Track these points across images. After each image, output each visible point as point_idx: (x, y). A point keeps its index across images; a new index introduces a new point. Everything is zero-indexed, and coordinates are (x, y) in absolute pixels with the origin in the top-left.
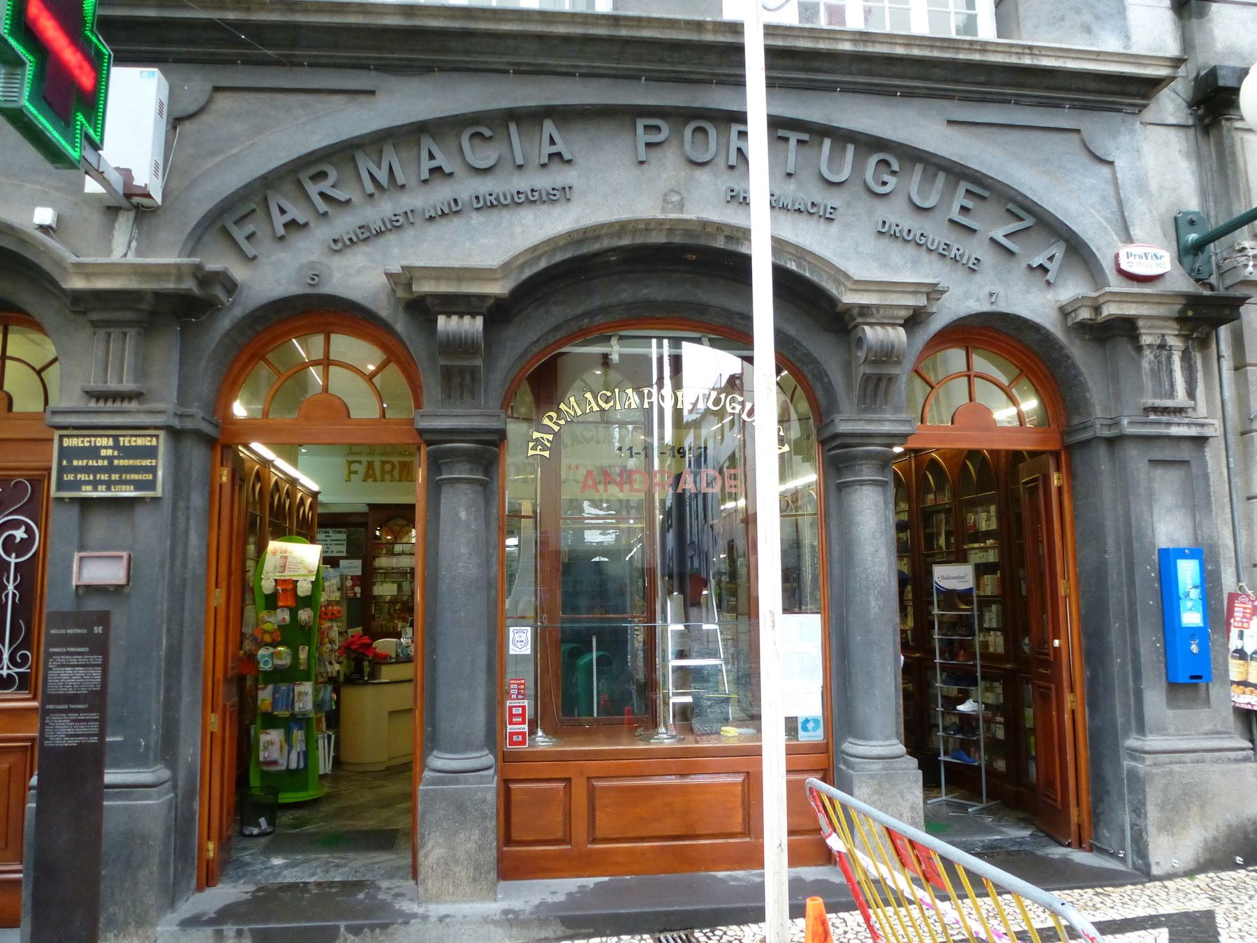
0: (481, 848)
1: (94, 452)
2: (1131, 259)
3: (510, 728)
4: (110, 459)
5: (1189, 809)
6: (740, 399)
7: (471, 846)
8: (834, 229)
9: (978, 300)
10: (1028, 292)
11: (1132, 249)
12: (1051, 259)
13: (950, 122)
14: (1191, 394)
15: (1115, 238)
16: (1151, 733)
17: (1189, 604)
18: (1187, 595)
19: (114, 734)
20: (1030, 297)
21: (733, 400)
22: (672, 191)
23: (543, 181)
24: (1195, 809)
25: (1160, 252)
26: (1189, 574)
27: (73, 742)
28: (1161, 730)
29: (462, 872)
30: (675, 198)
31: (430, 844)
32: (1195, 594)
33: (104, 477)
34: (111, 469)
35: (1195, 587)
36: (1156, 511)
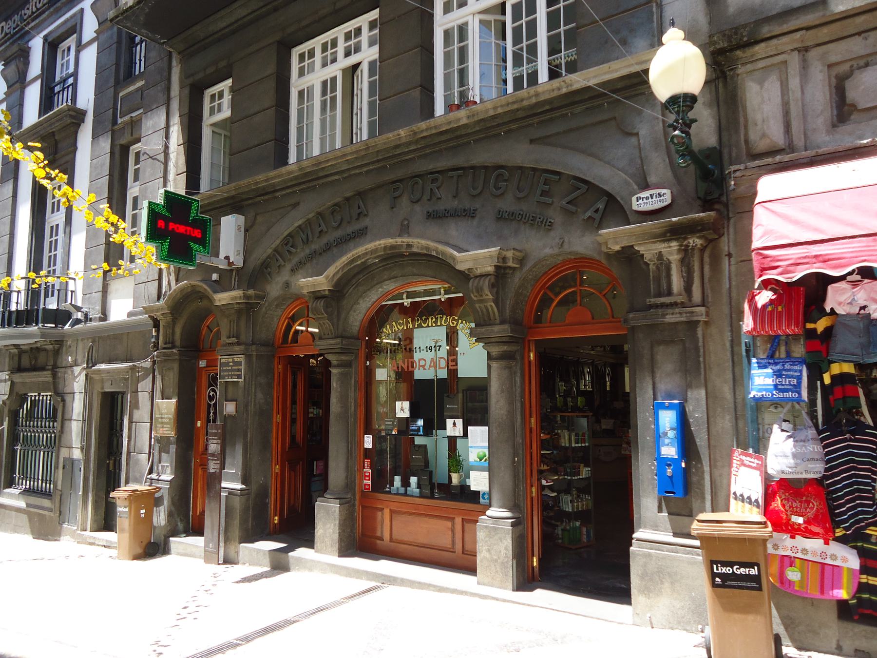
0: (334, 532)
1: (227, 364)
2: (640, 202)
3: (365, 482)
5: (662, 583)
7: (331, 531)
8: (475, 222)
9: (552, 247)
10: (583, 236)
12: (596, 211)
13: (532, 141)
14: (688, 289)
15: (635, 187)
16: (645, 527)
17: (667, 441)
18: (666, 434)
20: (584, 239)
22: (405, 219)
23: (356, 226)
24: (667, 585)
25: (663, 191)
26: (667, 419)
27: (213, 471)
28: (655, 527)
29: (328, 541)
30: (406, 223)
32: (671, 434)
34: (232, 370)
35: (672, 429)
36: (658, 375)
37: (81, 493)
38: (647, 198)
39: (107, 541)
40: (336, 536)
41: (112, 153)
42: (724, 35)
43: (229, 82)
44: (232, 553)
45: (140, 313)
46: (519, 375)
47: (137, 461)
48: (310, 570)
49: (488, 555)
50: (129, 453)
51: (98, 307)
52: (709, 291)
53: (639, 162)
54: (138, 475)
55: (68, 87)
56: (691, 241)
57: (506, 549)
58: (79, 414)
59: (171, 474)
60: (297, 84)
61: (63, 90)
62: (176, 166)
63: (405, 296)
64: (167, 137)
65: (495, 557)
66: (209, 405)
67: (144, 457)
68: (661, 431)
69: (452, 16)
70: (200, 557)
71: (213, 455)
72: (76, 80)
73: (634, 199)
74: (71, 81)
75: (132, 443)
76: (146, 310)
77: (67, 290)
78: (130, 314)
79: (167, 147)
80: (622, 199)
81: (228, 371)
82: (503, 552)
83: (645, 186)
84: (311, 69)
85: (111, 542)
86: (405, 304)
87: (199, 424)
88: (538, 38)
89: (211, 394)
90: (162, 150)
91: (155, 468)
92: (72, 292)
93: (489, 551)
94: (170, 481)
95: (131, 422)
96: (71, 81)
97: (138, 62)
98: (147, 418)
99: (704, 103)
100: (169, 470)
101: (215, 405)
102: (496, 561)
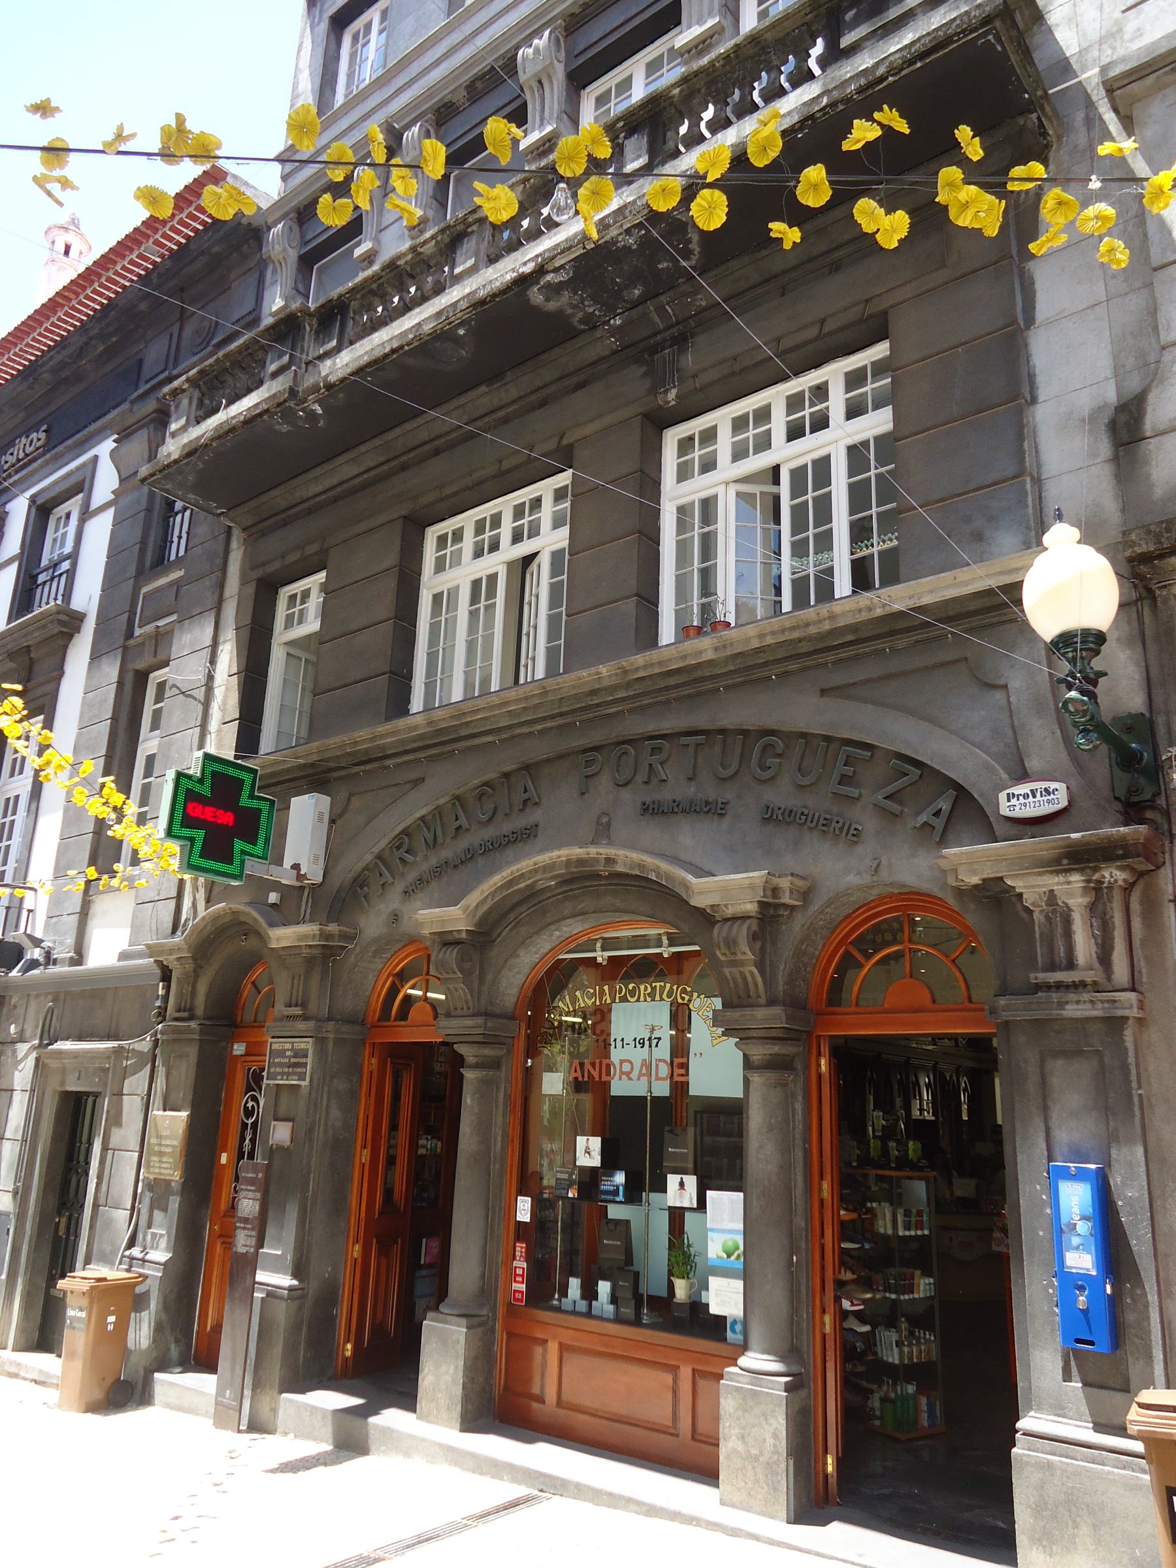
2: (1014, 801)
3: (515, 1286)
4: (290, 1057)
5: (1076, 1526)
6: (689, 989)
7: (449, 1378)
8: (726, 823)
9: (859, 873)
11: (1024, 789)
12: (937, 814)
13: (823, 692)
14: (1105, 958)
15: (1005, 776)
16: (1039, 1409)
17: (1075, 1241)
19: (270, 1247)
21: (684, 991)
24: (1085, 1530)
25: (1053, 785)
28: (1059, 1410)
30: (605, 820)
31: (426, 1370)
32: (1083, 1228)
33: (286, 1070)
35: (1084, 1218)
36: (1055, 1115)
37: (4, 1277)
38: (1026, 796)
39: (41, 1372)
40: (458, 1391)
41: (120, 684)
42: (1149, 532)
43: (321, 576)
44: (264, 1413)
45: (140, 955)
46: (800, 1098)
47: (109, 1223)
48: (407, 1454)
49: (740, 1447)
50: (96, 1206)
51: (70, 941)
52: (1143, 964)
53: (1010, 733)
54: (108, 1249)
55: (61, 575)
56: (1107, 875)
57: (775, 1436)
58: (16, 1130)
59: (167, 1250)
60: (430, 583)
61: (52, 579)
62: (223, 709)
63: (599, 945)
64: (213, 661)
65: (754, 1452)
66: (245, 1126)
67: (122, 1215)
68: (1064, 1220)
69: (689, 486)
70: (206, 1415)
71: (246, 1220)
72: (74, 565)
73: (1002, 796)
74: (66, 566)
75: (104, 1188)
76: (151, 950)
77: (20, 908)
78: (123, 956)
79: (210, 678)
80: (981, 795)
81: (281, 1065)
82: (770, 1441)
83: (1023, 776)
84: (457, 560)
85: (47, 1375)
86: (599, 960)
87: (224, 1158)
88: (835, 524)
89: (250, 1105)
90: (203, 682)
91: (140, 1236)
92: (30, 911)
93: (742, 1437)
94: (165, 1264)
95: (105, 1148)
96: (66, 566)
97: (175, 539)
98: (134, 1144)
99: (1118, 639)
100: (163, 1243)
101: (255, 1124)
102: (756, 1458)
